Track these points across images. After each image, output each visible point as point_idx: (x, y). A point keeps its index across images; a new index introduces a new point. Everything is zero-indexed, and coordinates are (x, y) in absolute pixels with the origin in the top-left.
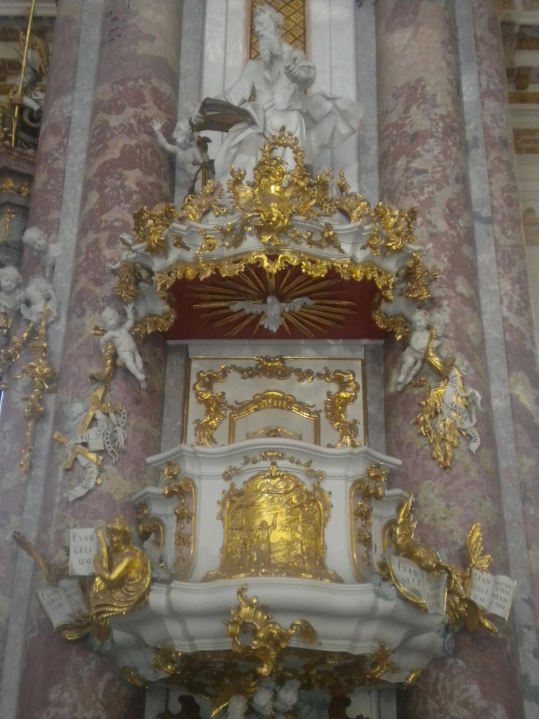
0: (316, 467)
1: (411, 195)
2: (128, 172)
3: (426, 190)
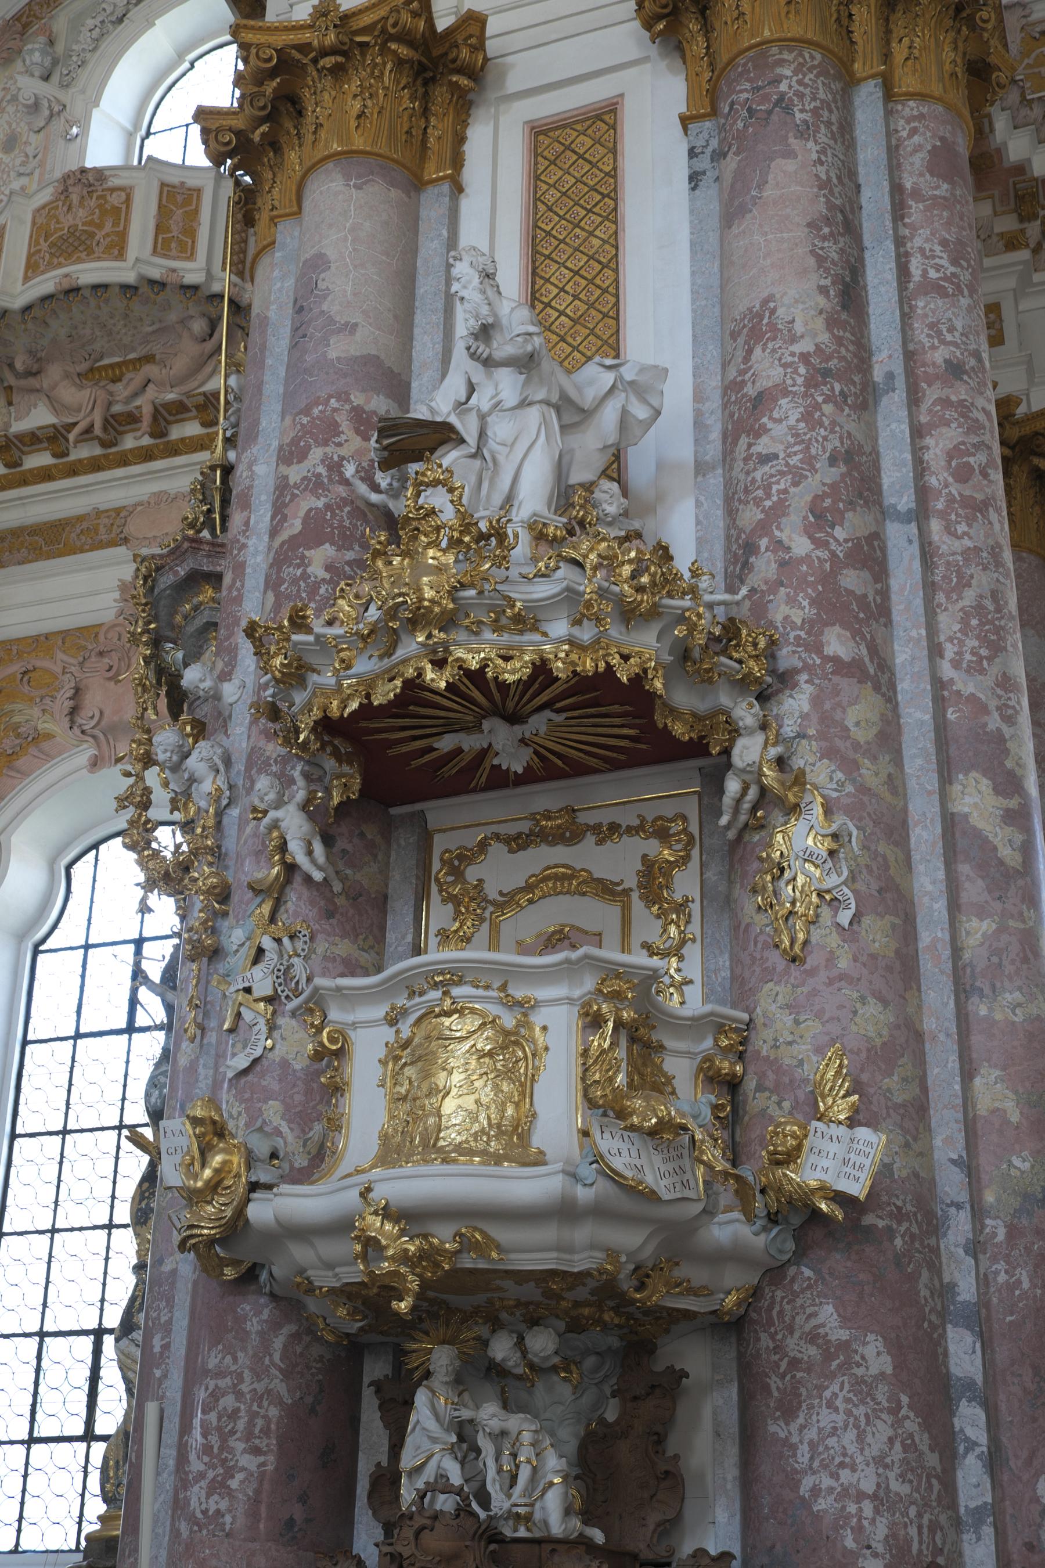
0: (519, 992)
3: (775, 488)
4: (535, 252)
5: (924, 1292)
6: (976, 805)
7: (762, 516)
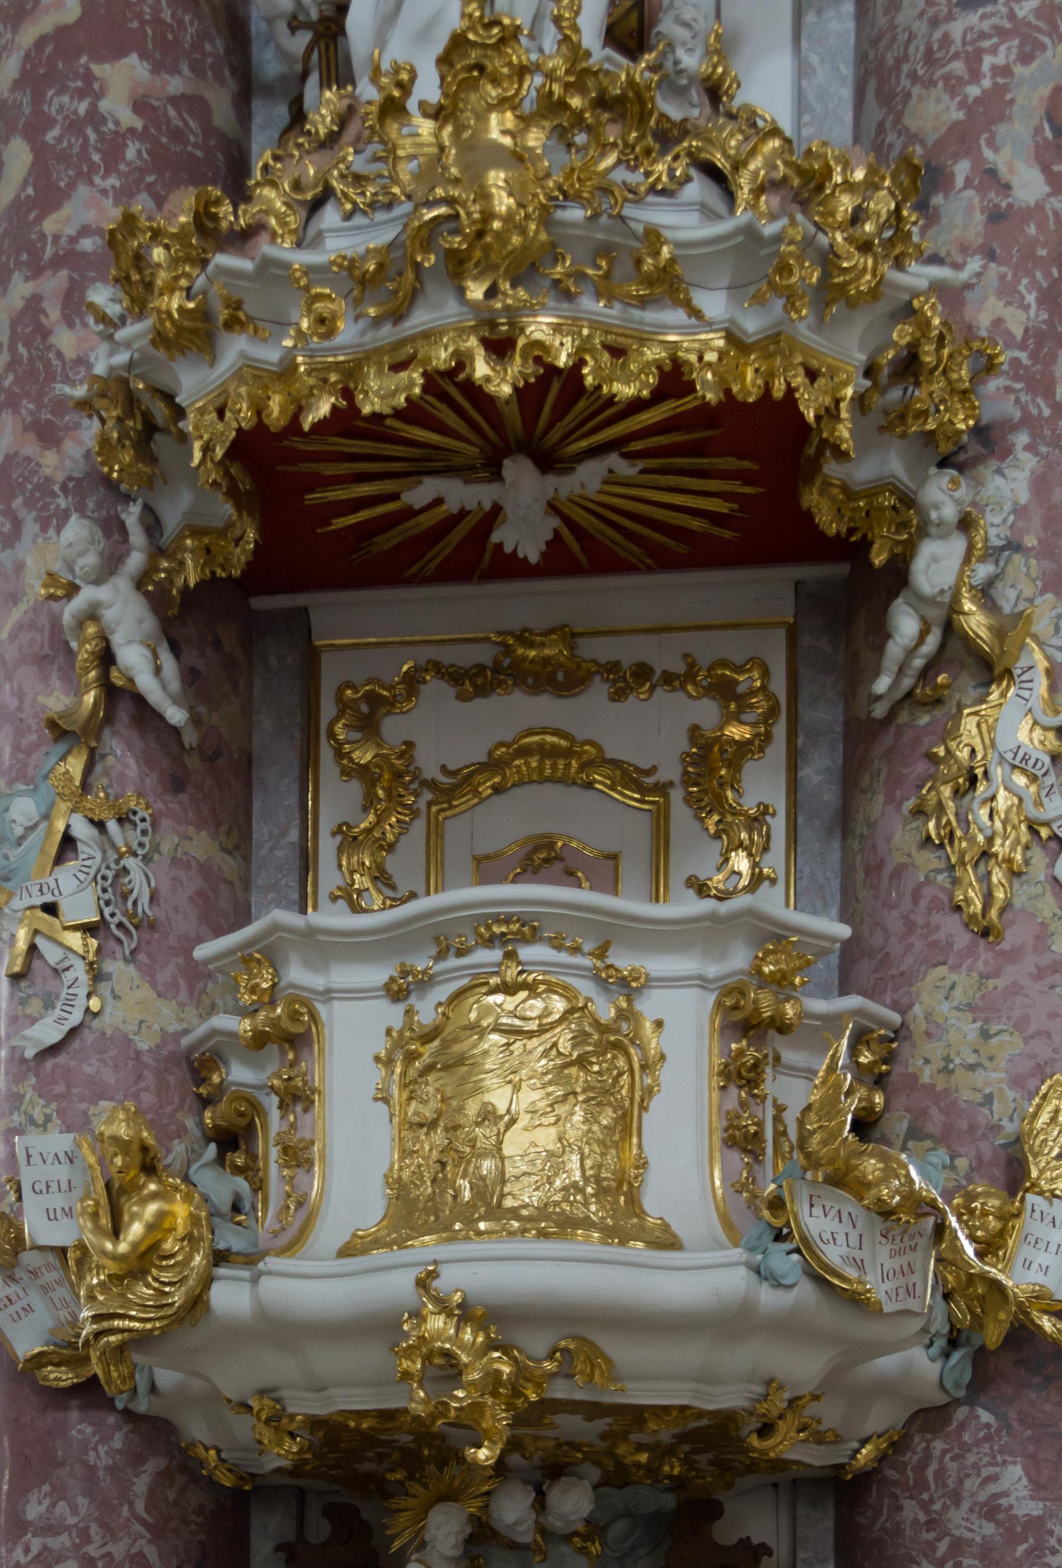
1: (940, 84)
2: (107, 67)
3: (988, 61)
7: (960, 115)
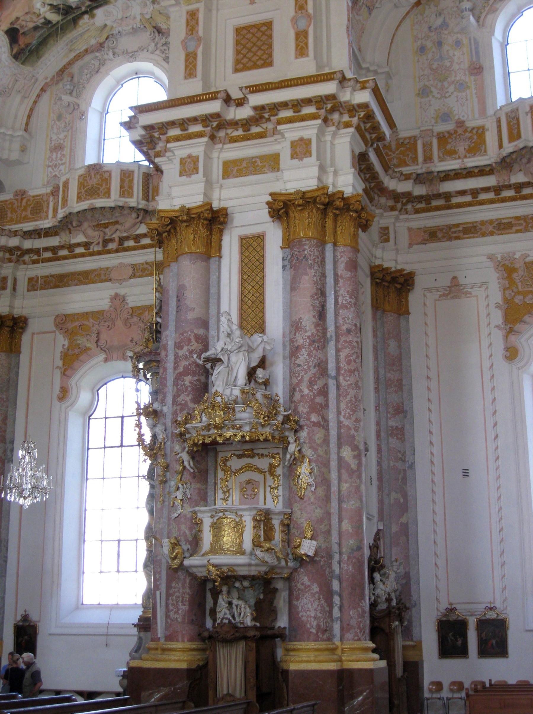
4: (242, 278)
5: (327, 573)
6: (347, 455)
